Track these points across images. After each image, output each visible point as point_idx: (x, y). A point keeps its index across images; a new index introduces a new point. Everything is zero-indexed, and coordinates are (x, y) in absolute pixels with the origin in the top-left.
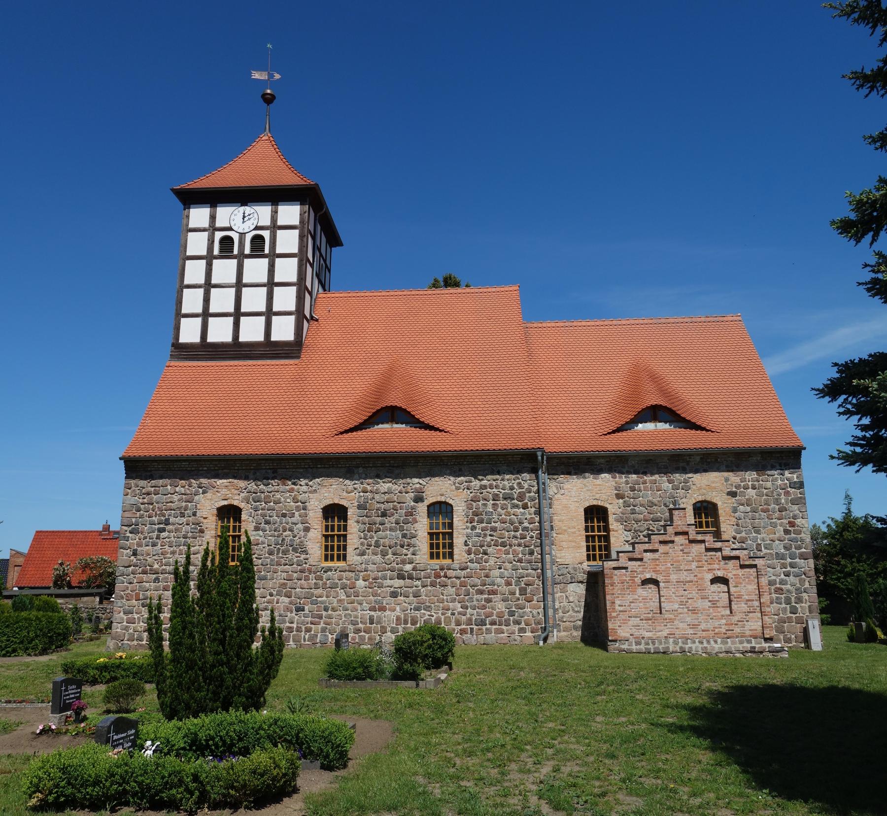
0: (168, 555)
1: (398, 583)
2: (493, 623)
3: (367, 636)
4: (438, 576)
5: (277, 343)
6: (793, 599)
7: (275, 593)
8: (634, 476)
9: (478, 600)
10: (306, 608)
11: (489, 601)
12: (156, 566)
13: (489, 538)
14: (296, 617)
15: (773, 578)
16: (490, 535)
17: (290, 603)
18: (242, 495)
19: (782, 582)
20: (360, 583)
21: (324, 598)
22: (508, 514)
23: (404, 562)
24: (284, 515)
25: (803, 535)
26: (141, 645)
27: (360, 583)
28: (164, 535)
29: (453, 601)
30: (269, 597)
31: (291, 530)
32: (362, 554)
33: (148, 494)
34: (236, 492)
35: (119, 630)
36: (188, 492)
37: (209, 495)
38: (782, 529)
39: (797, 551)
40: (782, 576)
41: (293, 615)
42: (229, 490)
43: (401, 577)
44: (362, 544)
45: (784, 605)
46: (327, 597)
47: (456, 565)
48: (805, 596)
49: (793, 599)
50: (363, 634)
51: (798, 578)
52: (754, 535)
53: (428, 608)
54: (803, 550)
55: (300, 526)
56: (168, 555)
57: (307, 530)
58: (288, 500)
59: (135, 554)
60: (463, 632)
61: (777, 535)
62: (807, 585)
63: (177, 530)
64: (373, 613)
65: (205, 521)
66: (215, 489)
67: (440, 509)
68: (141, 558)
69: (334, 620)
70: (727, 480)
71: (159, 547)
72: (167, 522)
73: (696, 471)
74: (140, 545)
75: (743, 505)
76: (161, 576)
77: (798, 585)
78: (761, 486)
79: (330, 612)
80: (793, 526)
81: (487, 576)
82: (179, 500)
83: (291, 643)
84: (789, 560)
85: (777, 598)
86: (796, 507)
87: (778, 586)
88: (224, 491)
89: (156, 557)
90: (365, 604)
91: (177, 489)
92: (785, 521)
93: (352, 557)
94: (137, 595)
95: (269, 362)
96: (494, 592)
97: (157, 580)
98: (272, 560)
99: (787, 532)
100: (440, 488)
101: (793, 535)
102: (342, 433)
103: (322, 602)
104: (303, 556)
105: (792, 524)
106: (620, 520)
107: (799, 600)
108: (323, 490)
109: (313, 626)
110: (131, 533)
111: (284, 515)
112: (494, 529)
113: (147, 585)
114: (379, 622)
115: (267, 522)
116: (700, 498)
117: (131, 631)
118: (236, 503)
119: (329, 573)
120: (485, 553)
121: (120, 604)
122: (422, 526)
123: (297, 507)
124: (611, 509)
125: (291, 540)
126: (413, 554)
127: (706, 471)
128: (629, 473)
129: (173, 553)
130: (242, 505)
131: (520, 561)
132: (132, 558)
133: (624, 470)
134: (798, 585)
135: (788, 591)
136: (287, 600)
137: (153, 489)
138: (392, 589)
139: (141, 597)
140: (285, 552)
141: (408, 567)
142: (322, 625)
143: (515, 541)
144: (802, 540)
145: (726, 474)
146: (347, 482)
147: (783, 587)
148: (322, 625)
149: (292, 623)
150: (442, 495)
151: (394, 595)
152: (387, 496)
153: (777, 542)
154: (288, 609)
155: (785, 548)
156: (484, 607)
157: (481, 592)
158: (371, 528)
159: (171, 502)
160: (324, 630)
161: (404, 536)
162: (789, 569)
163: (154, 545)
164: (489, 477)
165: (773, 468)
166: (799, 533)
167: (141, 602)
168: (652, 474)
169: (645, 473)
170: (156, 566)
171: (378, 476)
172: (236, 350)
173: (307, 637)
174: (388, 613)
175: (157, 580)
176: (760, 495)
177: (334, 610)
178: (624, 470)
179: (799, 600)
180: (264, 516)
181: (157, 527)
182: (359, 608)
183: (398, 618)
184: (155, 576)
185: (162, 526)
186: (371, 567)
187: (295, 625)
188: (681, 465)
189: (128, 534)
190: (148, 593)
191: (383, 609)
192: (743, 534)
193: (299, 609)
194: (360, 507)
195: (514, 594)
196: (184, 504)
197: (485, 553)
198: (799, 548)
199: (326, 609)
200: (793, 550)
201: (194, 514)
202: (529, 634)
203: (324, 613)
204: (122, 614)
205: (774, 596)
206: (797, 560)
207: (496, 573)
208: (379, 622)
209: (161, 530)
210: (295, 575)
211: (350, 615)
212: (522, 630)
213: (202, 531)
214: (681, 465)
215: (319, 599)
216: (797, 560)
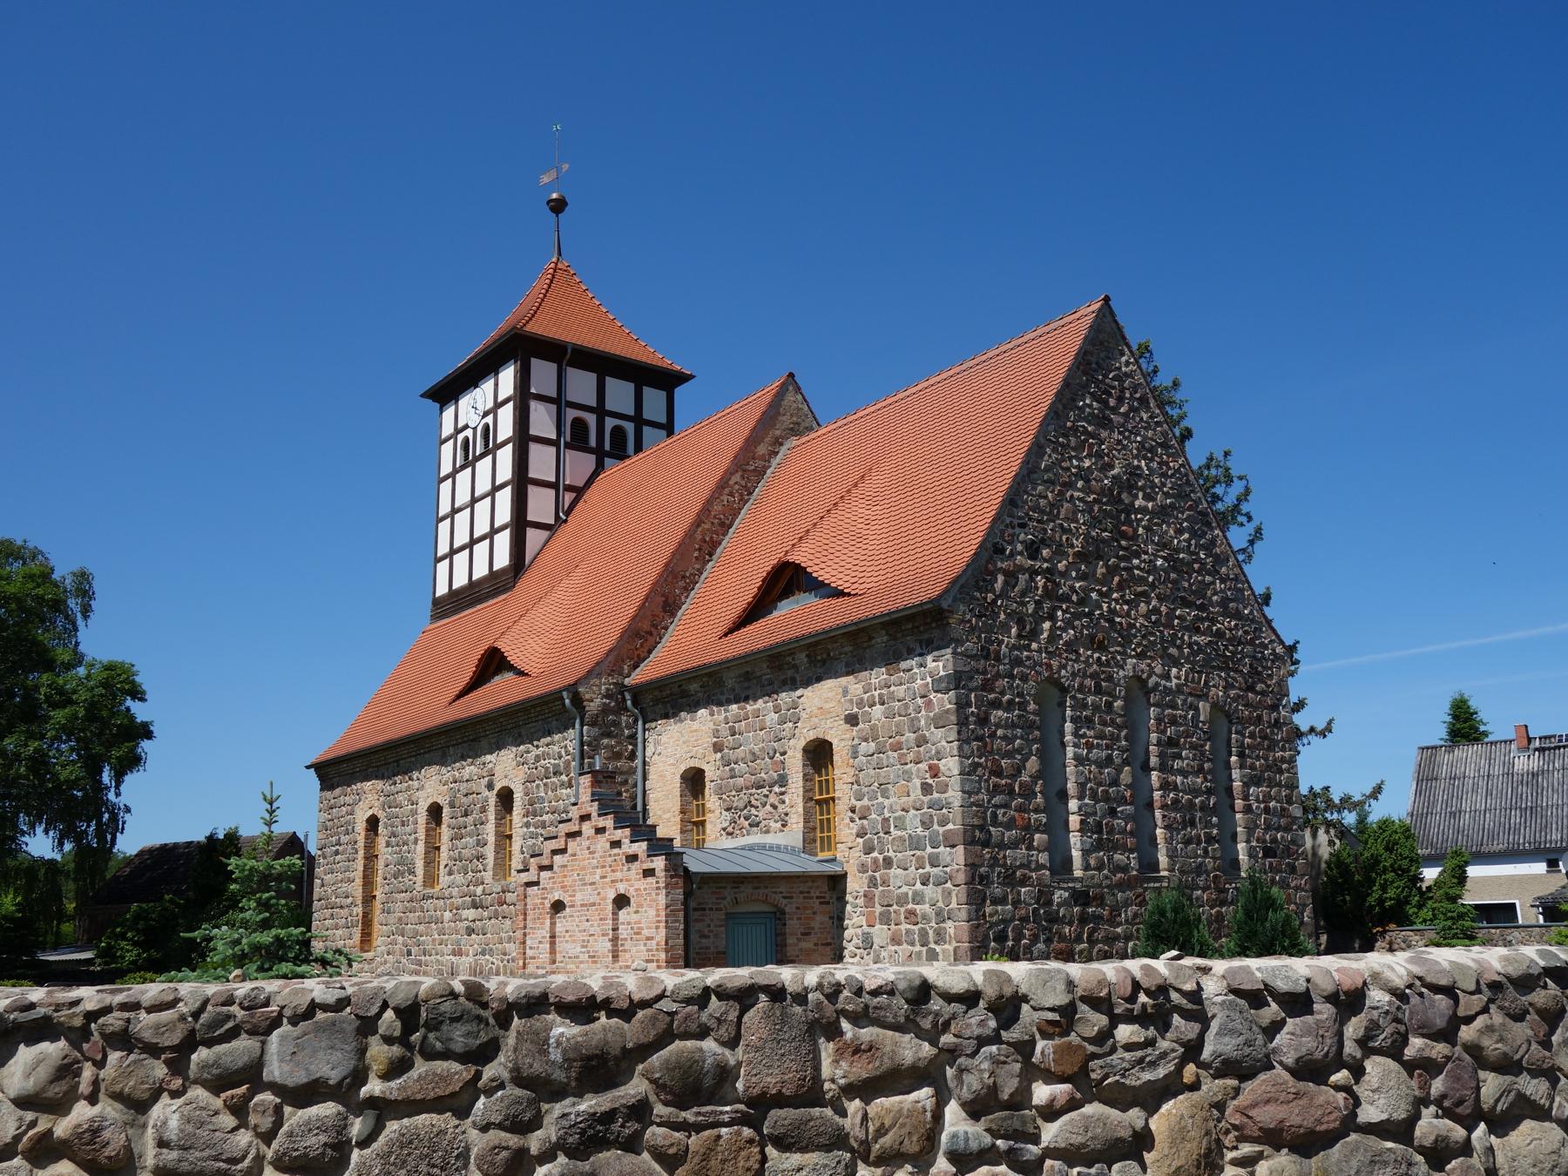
1: (471, 913)
6: (931, 932)
8: (734, 707)
15: (905, 889)
19: (918, 898)
25: (950, 793)
27: (447, 915)
29: (510, 940)
32: (450, 874)
38: (917, 782)
39: (941, 830)
40: (918, 886)
43: (475, 906)
45: (918, 948)
48: (950, 927)
49: (931, 932)
51: (939, 889)
52: (881, 800)
54: (950, 826)
61: (912, 797)
62: (954, 905)
70: (845, 692)
73: (807, 683)
75: (866, 740)
77: (940, 904)
78: (892, 697)
80: (935, 776)
84: (929, 850)
85: (908, 931)
86: (939, 733)
87: (910, 906)
92: (924, 766)
95: (491, 602)
99: (927, 789)
101: (936, 795)
105: (935, 772)
106: (720, 792)
107: (940, 937)
116: (812, 736)
124: (709, 775)
127: (819, 680)
128: (729, 702)
133: (723, 698)
134: (940, 904)
135: (924, 917)
141: (479, 890)
144: (948, 805)
145: (843, 680)
146: (444, 770)
147: (918, 907)
153: (913, 812)
155: (923, 823)
162: (928, 868)
165: (910, 653)
166: (944, 788)
168: (755, 700)
169: (746, 699)
171: (463, 758)
176: (890, 715)
178: (723, 698)
179: (940, 937)
186: (455, 891)
188: (790, 673)
192: (865, 802)
198: (943, 823)
200: (935, 827)
205: (904, 927)
206: (942, 848)
214: (790, 673)
216: (942, 848)
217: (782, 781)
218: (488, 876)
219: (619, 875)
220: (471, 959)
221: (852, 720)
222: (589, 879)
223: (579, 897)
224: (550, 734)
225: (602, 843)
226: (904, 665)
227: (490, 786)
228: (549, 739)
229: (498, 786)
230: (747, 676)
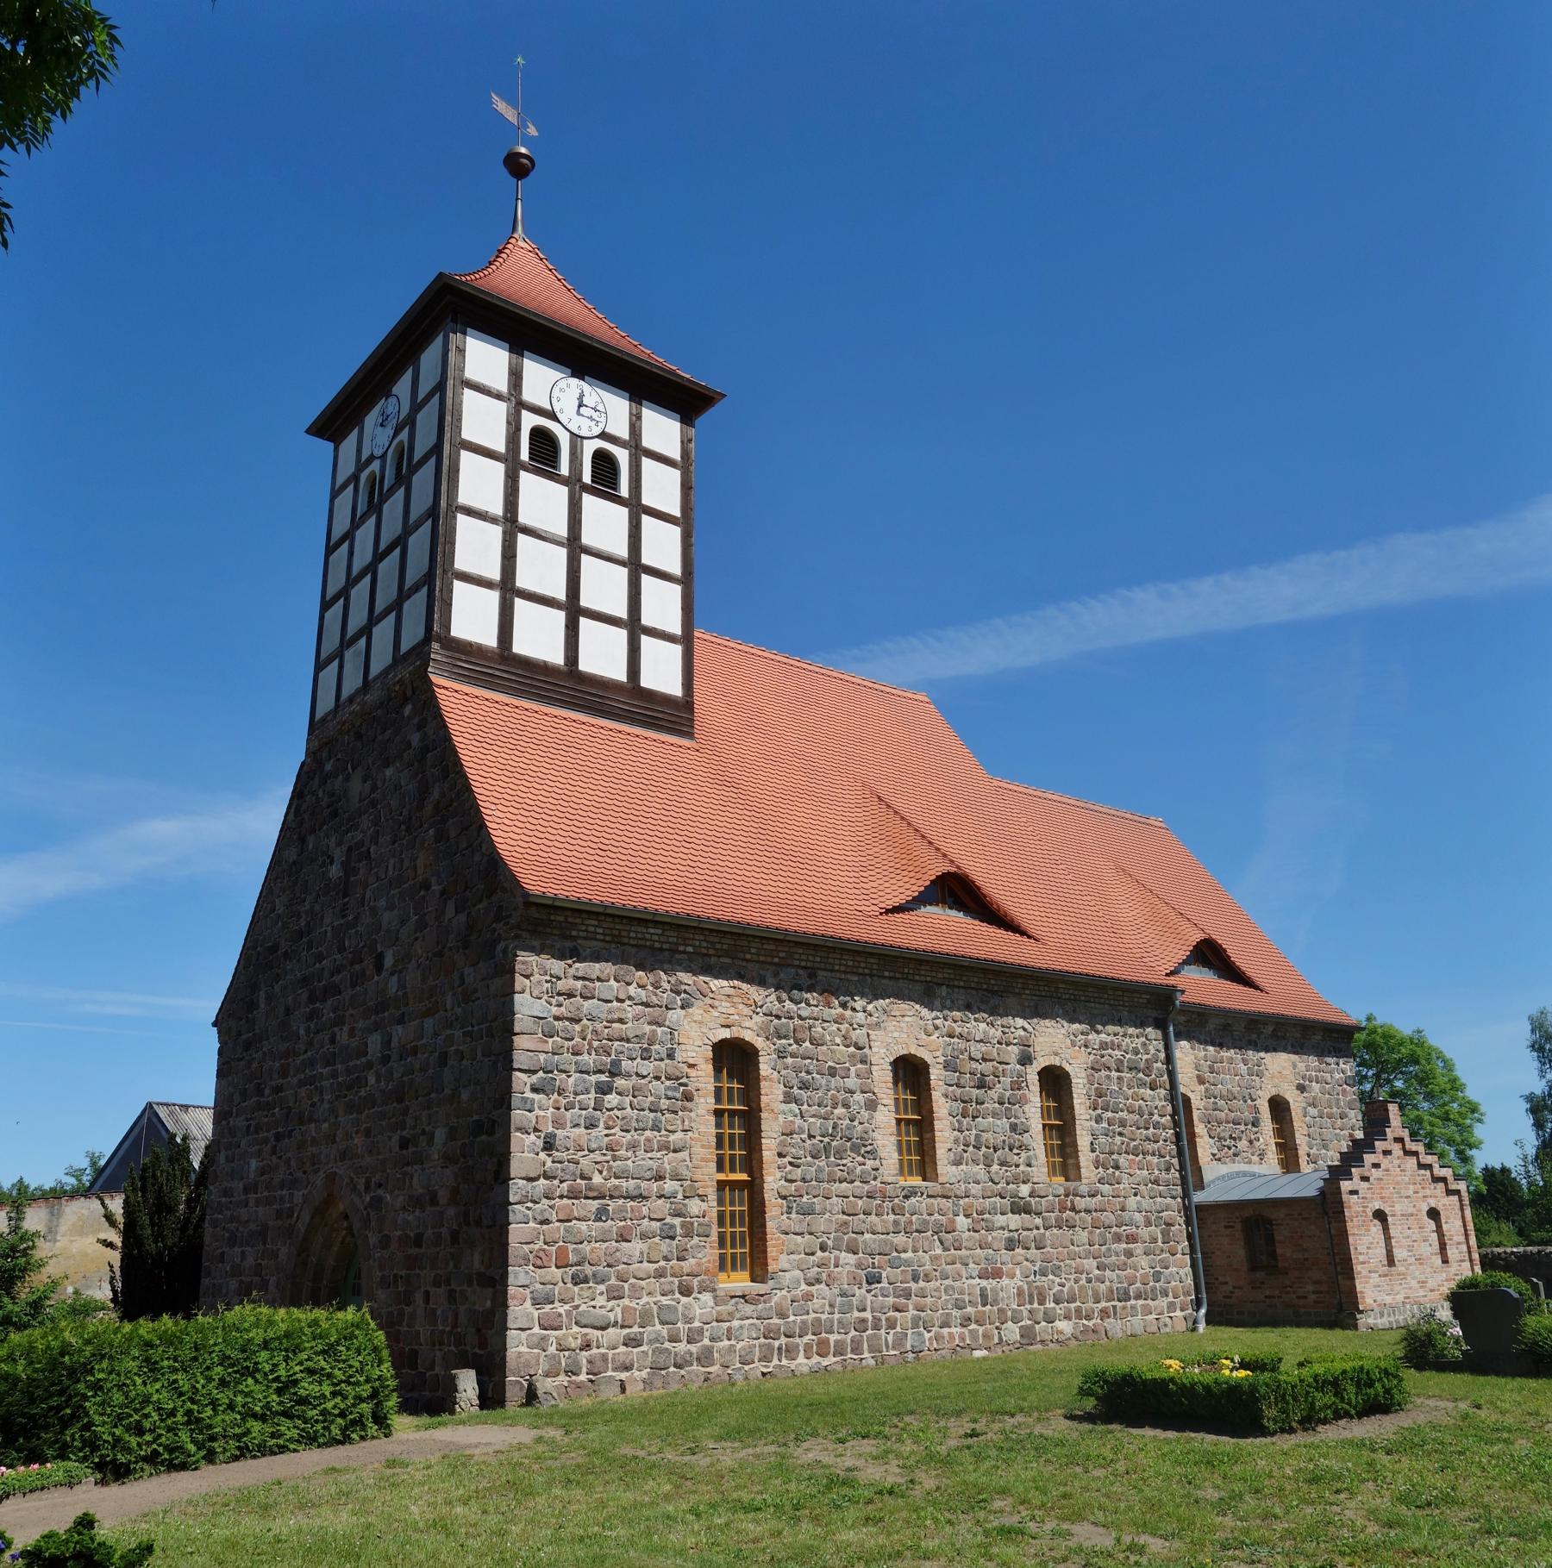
0: (622, 1153)
1: (1014, 1221)
2: (1138, 1297)
3: (981, 1330)
4: (1063, 1209)
5: (651, 696)
7: (830, 1243)
8: (1211, 1048)
9: (1117, 1254)
10: (884, 1275)
11: (1129, 1254)
12: (597, 1179)
13: (1118, 1138)
14: (869, 1297)
16: (1120, 1134)
17: (859, 1266)
18: (757, 1019)
20: (962, 1222)
21: (910, 1254)
22: (1135, 1097)
23: (1016, 1180)
24: (832, 1072)
26: (579, 1386)
27: (962, 1222)
28: (612, 1099)
30: (819, 1253)
31: (846, 1106)
32: (957, 1163)
33: (570, 995)
34: (747, 1011)
35: (523, 1349)
36: (655, 1000)
37: (696, 1011)
41: (863, 1291)
42: (734, 1005)
43: (1017, 1209)
44: (956, 1141)
46: (915, 1251)
47: (1084, 1189)
50: (973, 1326)
53: (1056, 1271)
55: (858, 1097)
56: (622, 1153)
57: (872, 1105)
58: (838, 1040)
59: (549, 1146)
60: (1104, 1313)
63: (635, 1092)
64: (984, 1283)
65: (692, 1072)
66: (708, 1001)
67: (1055, 1082)
68: (564, 1156)
69: (929, 1300)
70: (1295, 1066)
71: (601, 1130)
72: (615, 1072)
74: (559, 1124)
76: (612, 1205)
79: (922, 1284)
81: (1123, 1210)
82: (637, 1018)
83: (866, 1355)
88: (724, 1006)
89: (597, 1156)
90: (972, 1265)
91: (632, 990)
93: (946, 1169)
94: (562, 1253)
96: (1132, 1239)
97: (601, 1215)
98: (820, 1170)
100: (1056, 1040)
102: (888, 912)
103: (908, 1263)
104: (870, 1163)
108: (891, 1025)
109: (897, 1314)
110: (535, 1090)
111: (832, 1072)
112: (1123, 1123)
113: (583, 1226)
114: (995, 1302)
115: (804, 1086)
117: (552, 1349)
118: (748, 1036)
119: (913, 1200)
120: (1117, 1167)
121: (523, 1280)
122: (1033, 1110)
123: (852, 1056)
125: (848, 1128)
126: (1029, 1165)
127: (1275, 1050)
128: (1206, 1043)
129: (633, 1146)
130: (759, 1042)
131: (1156, 1182)
132: (542, 1155)
136: (850, 1259)
137: (579, 984)
138: (1007, 1234)
139: (572, 1258)
140: (840, 1154)
141: (1024, 1190)
142: (912, 1312)
143: (1150, 1147)
148: (912, 1312)
149: (864, 1310)
150: (1056, 1054)
151: (1011, 1245)
152: (983, 1048)
154: (855, 1281)
156: (1123, 1267)
157: (1118, 1238)
158: (967, 1110)
159: (621, 1021)
160: (915, 1322)
161: (1014, 1128)
163: (591, 1125)
164: (1110, 1028)
167: (571, 1271)
169: (1221, 1046)
170: (597, 1179)
171: (968, 1007)
172: (566, 686)
173: (890, 1338)
174: (1005, 1281)
175: (601, 1215)
177: (927, 1279)
180: (797, 1070)
181: (593, 1078)
182: (964, 1274)
183: (1020, 1293)
184: (595, 1204)
185: (603, 1078)
186: (975, 1189)
187: (868, 1315)
188: (1254, 1037)
189: (529, 1094)
190: (586, 1247)
191: (997, 1274)
193: (873, 1280)
194: (947, 1066)
195: (1155, 1241)
196: (648, 1028)
197: (1117, 1167)
199: (915, 1279)
201: (671, 1056)
202: (1178, 1313)
203: (913, 1285)
204: (528, 1303)
207: (1132, 1202)
208: (995, 1302)
209: (604, 1089)
210: (860, 1202)
211: (953, 1288)
212: (1171, 1307)
213: (688, 1097)
215: (903, 1255)
217: (1255, 1123)
218: (1040, 1171)
219: (1428, 1192)
220: (1018, 1281)
221: (1301, 1088)
222: (1404, 1193)
223: (1398, 1208)
224: (1120, 1023)
225: (1413, 1161)
226: (1329, 1060)
227: (1026, 1060)
228: (1117, 1029)
229: (1041, 1062)
230: (1226, 1028)
